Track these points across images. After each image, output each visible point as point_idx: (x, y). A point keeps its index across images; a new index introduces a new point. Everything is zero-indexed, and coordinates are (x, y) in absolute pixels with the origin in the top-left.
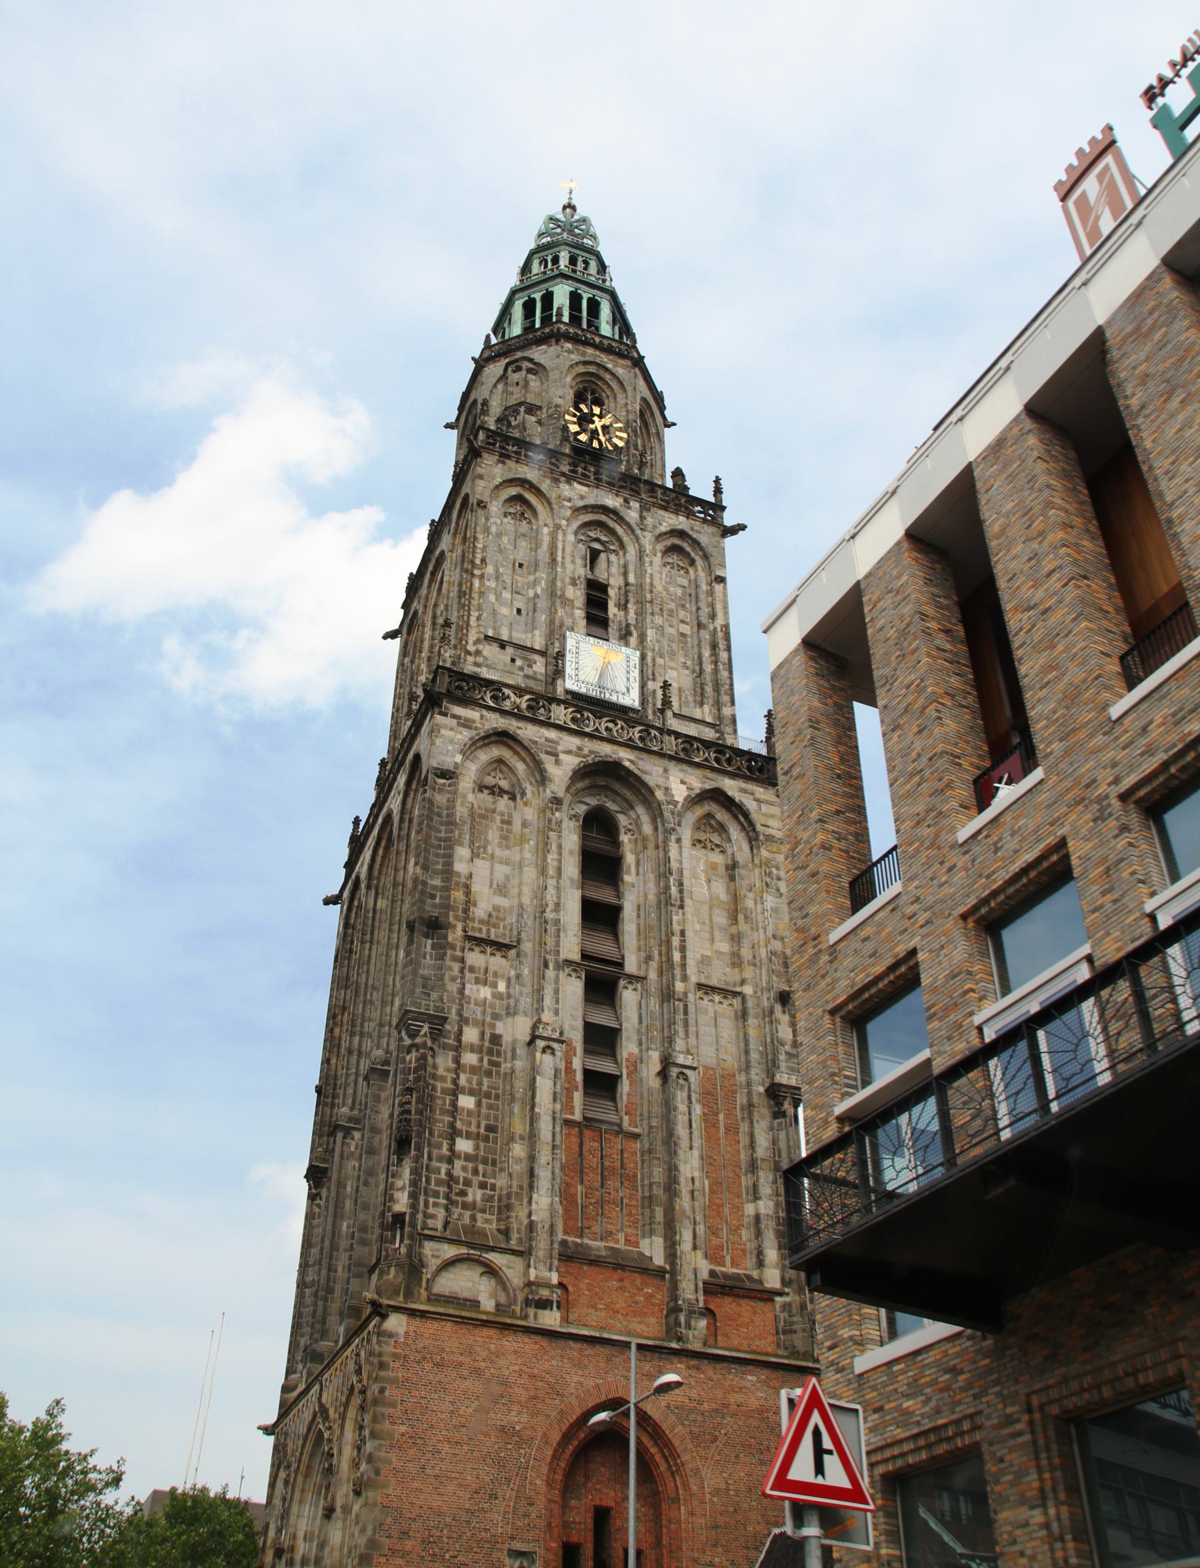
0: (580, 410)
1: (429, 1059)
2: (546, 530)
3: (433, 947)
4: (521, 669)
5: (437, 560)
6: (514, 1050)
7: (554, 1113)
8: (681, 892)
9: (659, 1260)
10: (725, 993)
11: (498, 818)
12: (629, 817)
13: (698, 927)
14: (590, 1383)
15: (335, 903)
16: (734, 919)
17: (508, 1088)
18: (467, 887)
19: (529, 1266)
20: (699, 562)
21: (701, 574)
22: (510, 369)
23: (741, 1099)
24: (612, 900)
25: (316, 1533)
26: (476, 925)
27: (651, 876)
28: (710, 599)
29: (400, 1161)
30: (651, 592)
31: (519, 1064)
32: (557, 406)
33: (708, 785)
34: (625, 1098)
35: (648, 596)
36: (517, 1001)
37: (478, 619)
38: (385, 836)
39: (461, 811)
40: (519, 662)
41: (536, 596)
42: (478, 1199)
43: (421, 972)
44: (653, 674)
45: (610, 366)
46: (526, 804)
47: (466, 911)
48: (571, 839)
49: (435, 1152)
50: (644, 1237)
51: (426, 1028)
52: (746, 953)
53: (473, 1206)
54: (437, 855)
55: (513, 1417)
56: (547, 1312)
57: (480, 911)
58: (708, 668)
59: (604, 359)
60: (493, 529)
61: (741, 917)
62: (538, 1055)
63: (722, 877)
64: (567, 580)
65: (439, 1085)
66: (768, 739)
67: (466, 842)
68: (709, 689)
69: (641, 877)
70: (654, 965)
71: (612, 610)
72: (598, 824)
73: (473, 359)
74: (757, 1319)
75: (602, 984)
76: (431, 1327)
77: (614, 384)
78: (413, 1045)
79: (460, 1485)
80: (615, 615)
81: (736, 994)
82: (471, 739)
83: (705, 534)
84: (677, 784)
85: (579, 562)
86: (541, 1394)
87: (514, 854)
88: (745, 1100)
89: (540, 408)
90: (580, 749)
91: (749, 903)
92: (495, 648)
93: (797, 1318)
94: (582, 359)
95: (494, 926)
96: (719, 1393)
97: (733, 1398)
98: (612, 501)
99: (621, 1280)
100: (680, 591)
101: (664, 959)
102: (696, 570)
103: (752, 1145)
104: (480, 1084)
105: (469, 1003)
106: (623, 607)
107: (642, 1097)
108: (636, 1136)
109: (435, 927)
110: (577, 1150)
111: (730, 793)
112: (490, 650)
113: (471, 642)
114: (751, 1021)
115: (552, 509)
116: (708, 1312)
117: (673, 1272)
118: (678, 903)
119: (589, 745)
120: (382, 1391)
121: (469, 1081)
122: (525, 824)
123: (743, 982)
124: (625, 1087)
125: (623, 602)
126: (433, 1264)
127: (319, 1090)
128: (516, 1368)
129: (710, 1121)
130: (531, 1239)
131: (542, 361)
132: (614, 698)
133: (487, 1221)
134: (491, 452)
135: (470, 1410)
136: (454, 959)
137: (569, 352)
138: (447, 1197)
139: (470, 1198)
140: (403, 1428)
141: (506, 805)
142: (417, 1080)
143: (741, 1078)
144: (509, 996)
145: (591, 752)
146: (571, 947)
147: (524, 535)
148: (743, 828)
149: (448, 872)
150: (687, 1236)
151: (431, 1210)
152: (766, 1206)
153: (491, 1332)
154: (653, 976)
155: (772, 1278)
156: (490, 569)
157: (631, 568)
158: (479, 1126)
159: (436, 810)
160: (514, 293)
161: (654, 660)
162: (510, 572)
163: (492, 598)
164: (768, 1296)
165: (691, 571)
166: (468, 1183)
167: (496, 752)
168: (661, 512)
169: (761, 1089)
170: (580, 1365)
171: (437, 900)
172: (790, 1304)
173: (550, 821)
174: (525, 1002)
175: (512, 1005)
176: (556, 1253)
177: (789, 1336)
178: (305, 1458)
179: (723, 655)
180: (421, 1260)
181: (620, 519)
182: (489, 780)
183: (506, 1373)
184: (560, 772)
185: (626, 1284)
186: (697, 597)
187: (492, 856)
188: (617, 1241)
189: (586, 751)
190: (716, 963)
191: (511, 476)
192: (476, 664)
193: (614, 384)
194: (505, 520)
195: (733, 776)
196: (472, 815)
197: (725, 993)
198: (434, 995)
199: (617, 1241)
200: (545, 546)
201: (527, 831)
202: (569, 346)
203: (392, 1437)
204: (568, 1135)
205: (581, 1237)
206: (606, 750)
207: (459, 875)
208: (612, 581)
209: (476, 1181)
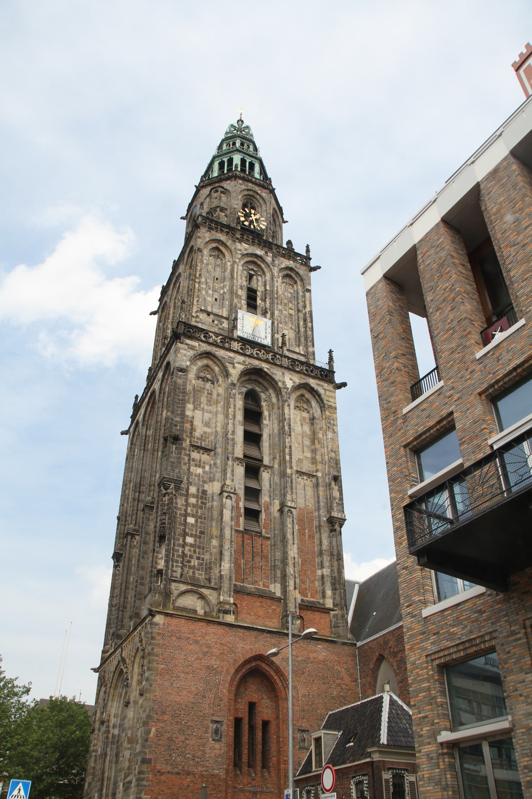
0: (245, 211)
1: (174, 499)
2: (229, 264)
3: (176, 449)
4: (217, 325)
5: (177, 277)
6: (213, 497)
7: (232, 526)
8: (290, 428)
9: (278, 594)
10: (310, 475)
11: (206, 392)
12: (266, 395)
13: (296, 445)
14: (248, 647)
15: (126, 434)
16: (313, 443)
17: (210, 514)
18: (192, 422)
19: (220, 595)
20: (299, 282)
21: (300, 288)
22: (213, 191)
23: (316, 523)
24: (258, 432)
25: (120, 714)
26: (196, 440)
27: (276, 421)
28: (303, 299)
29: (160, 546)
30: (277, 294)
31: (215, 503)
32: (234, 208)
34: (263, 521)
35: (276, 296)
36: (214, 475)
37: (198, 301)
38: (151, 402)
39: (189, 388)
40: (216, 322)
41: (224, 293)
42: (196, 564)
43: (170, 460)
44: (278, 331)
45: (259, 192)
46: (219, 386)
47: (191, 433)
48: (240, 403)
49: (176, 542)
50: (271, 584)
51: (172, 486)
52: (319, 458)
53: (194, 567)
54: (178, 407)
55: (213, 662)
56: (228, 615)
57: (198, 433)
58: (302, 330)
59: (257, 188)
60: (205, 262)
61: (316, 441)
62: (224, 499)
63: (308, 424)
64: (239, 287)
65: (178, 512)
66: (329, 362)
67: (192, 402)
68: (302, 339)
69: (271, 422)
70: (277, 461)
71: (259, 301)
72: (251, 397)
73: (195, 186)
74: (322, 621)
75: (253, 469)
76: (175, 621)
77: (261, 201)
78: (166, 493)
79: (189, 692)
80: (260, 304)
81: (313, 476)
82: (194, 355)
83: (302, 270)
84: (289, 380)
85: (244, 279)
86: (225, 652)
87: (213, 408)
88: (317, 524)
89: (226, 209)
90: (244, 362)
91: (320, 436)
92: (205, 315)
93: (340, 621)
94: (247, 188)
95: (204, 441)
96: (305, 653)
97: (312, 655)
98: (259, 252)
99: (262, 602)
100: (289, 295)
101: (282, 458)
102: (297, 286)
103: (321, 544)
104: (197, 512)
105: (192, 475)
106: (264, 300)
107: (271, 521)
108: (268, 538)
109: (176, 439)
110: (241, 543)
111: (312, 386)
112: (203, 316)
113: (194, 312)
114: (321, 488)
115: (232, 254)
116: (301, 618)
117: (285, 599)
118: (288, 434)
119: (248, 360)
120: (153, 649)
121: (192, 511)
122: (218, 395)
123: (317, 471)
124: (263, 516)
125: (264, 298)
126: (176, 593)
127: (118, 518)
128: (214, 640)
129: (301, 532)
130: (221, 583)
131: (228, 188)
132: (259, 341)
133: (200, 574)
134: (204, 226)
135: (193, 659)
136: (186, 455)
137: (241, 184)
138: (182, 563)
139: (192, 564)
140: (162, 666)
141: (210, 386)
142: (169, 509)
143: (316, 514)
144: (211, 473)
145: (249, 363)
146: (239, 452)
147: (219, 265)
148: (318, 401)
149: (183, 415)
150: (292, 583)
151: (175, 569)
152: (326, 571)
153: (203, 624)
154: (276, 466)
155: (329, 603)
156: (203, 280)
157: (268, 283)
158: (196, 531)
159: (178, 386)
160: (214, 158)
161: (278, 325)
162: (212, 282)
163: (204, 292)
164: (327, 611)
165: (295, 286)
166: (191, 557)
167: (205, 362)
168: (282, 259)
169: (325, 519)
170: (243, 639)
171: (178, 427)
172: (337, 615)
173: (230, 394)
174: (218, 475)
175: (212, 477)
176: (232, 589)
177: (336, 629)
178: (114, 681)
179: (309, 325)
180: (170, 591)
181: (263, 261)
182: (202, 375)
183: (210, 642)
184: (235, 372)
185: (264, 604)
186: (297, 298)
187: (203, 409)
188: (259, 585)
189: (247, 363)
190: (305, 462)
191: (213, 238)
192: (196, 322)
193: (261, 201)
194: (210, 258)
195: (314, 378)
196: (194, 389)
197: (310, 475)
198: (177, 471)
199: (259, 585)
200: (228, 271)
201: (219, 398)
202: (241, 181)
203: (158, 670)
204: (237, 537)
205: (243, 583)
206: (256, 363)
207: (188, 416)
208: (259, 288)
209: (195, 556)
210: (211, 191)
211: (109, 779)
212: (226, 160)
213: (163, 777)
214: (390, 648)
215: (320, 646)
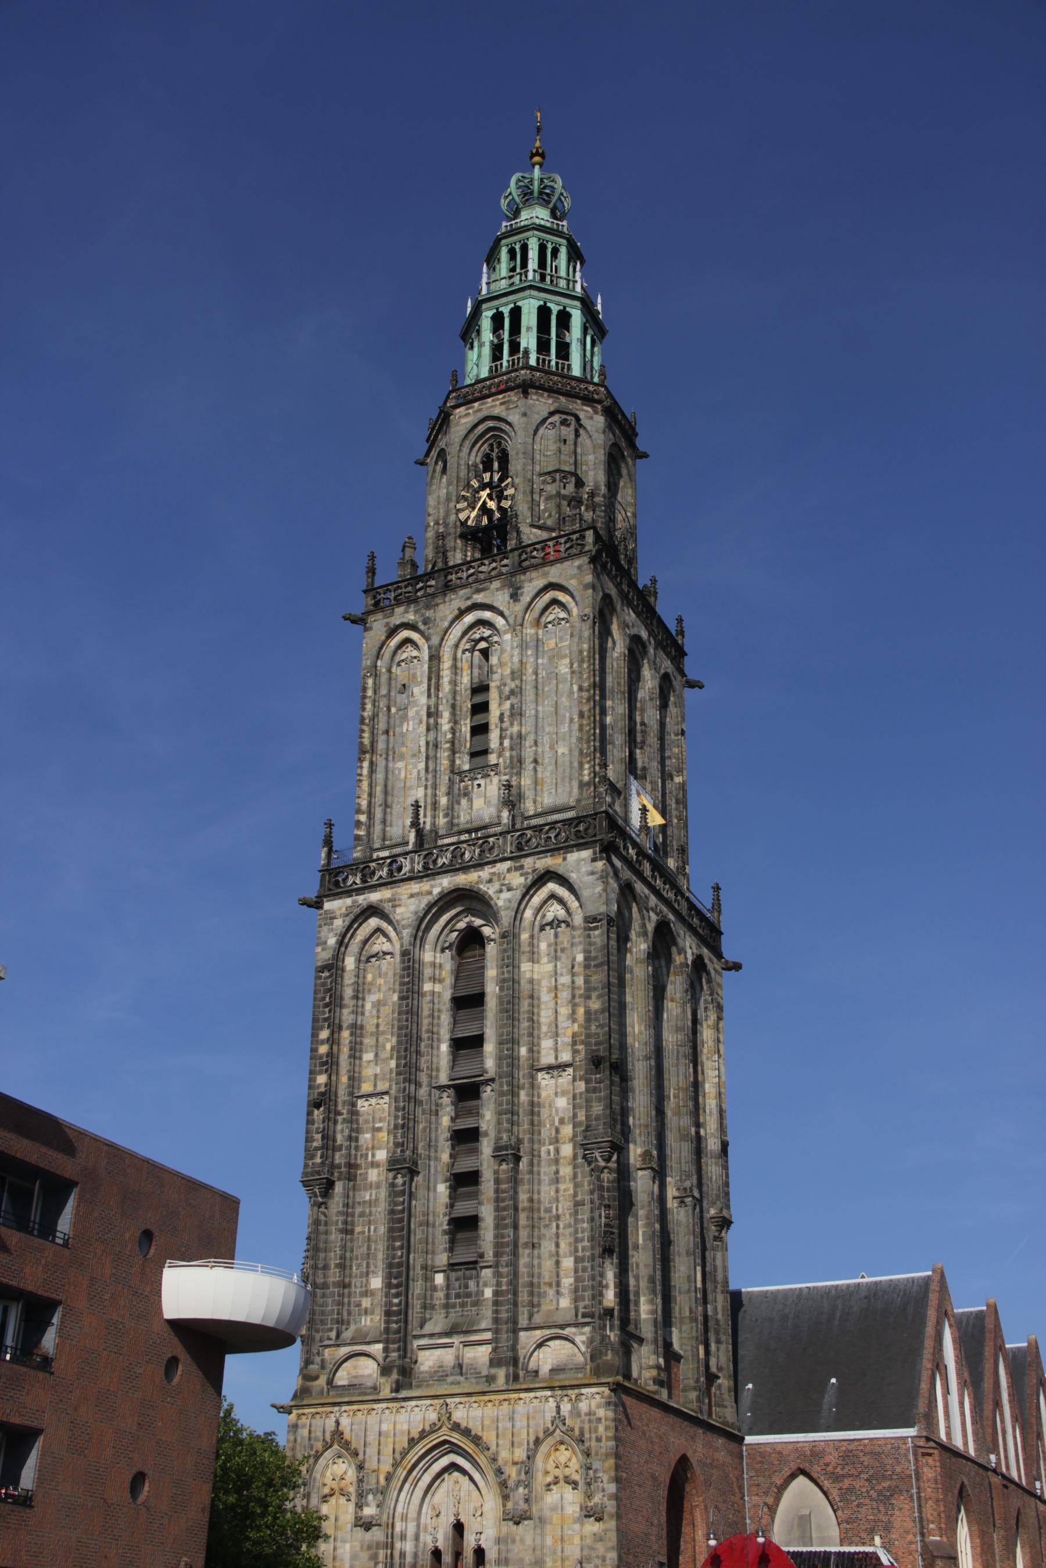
98: (644, 634)
210: (552, 414)
212: (555, 309)
214: (827, 1465)
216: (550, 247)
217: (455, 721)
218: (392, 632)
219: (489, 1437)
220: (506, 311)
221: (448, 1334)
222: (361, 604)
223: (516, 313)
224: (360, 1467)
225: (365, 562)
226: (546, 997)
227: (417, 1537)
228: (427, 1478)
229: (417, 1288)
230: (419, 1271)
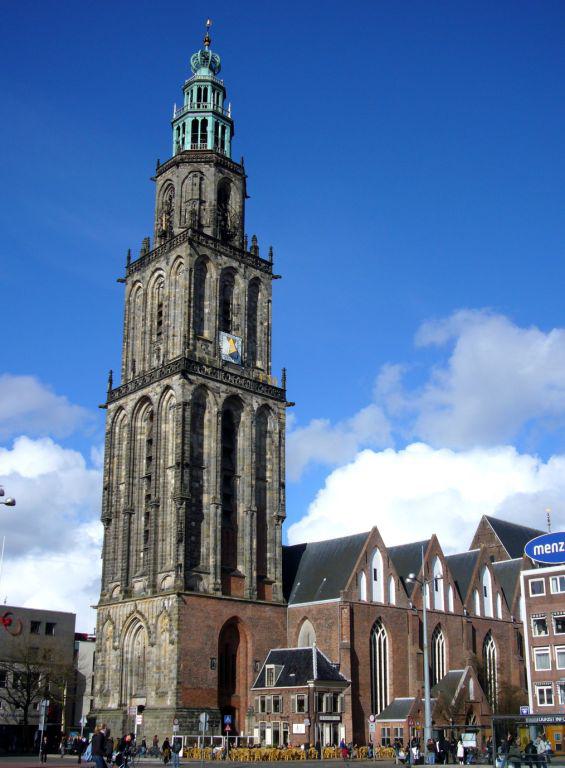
33: (264, 402)
59: (232, 175)
97: (263, 614)
98: (235, 264)
119: (230, 388)
211: (126, 685)
212: (200, 120)
213: (188, 691)
215: (268, 608)
216: (203, 88)
217: (152, 321)
218: (134, 284)
219: (146, 615)
220: (181, 125)
221: (142, 576)
222: (123, 273)
223: (184, 125)
224: (114, 628)
225: (127, 253)
226: (171, 438)
227: (132, 653)
228: (134, 631)
229: (133, 559)
230: (135, 553)
